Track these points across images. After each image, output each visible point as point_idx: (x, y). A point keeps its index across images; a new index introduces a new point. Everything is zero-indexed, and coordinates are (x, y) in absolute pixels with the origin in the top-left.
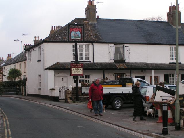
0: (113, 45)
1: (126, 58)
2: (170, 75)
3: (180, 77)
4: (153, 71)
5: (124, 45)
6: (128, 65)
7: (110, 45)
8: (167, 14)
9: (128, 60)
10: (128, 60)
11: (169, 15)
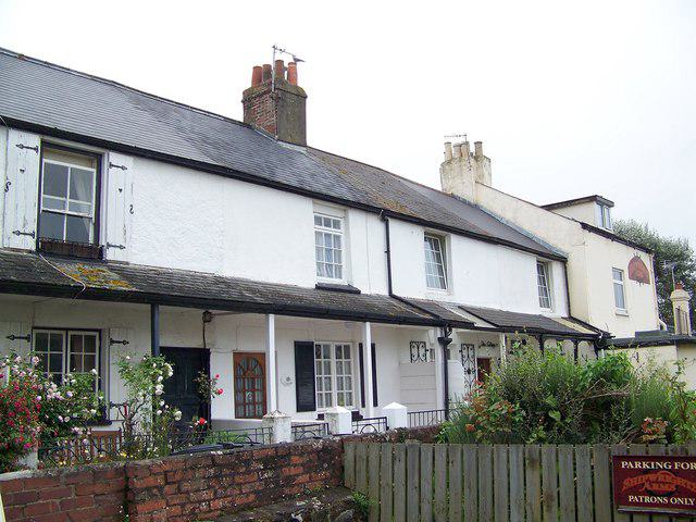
0: (34, 140)
1: (111, 233)
2: (338, 348)
3: (352, 360)
4: (272, 317)
5: (99, 158)
6: (123, 271)
7: (16, 137)
8: (242, 98)
9: (121, 247)
10: (121, 247)
11: (249, 100)
